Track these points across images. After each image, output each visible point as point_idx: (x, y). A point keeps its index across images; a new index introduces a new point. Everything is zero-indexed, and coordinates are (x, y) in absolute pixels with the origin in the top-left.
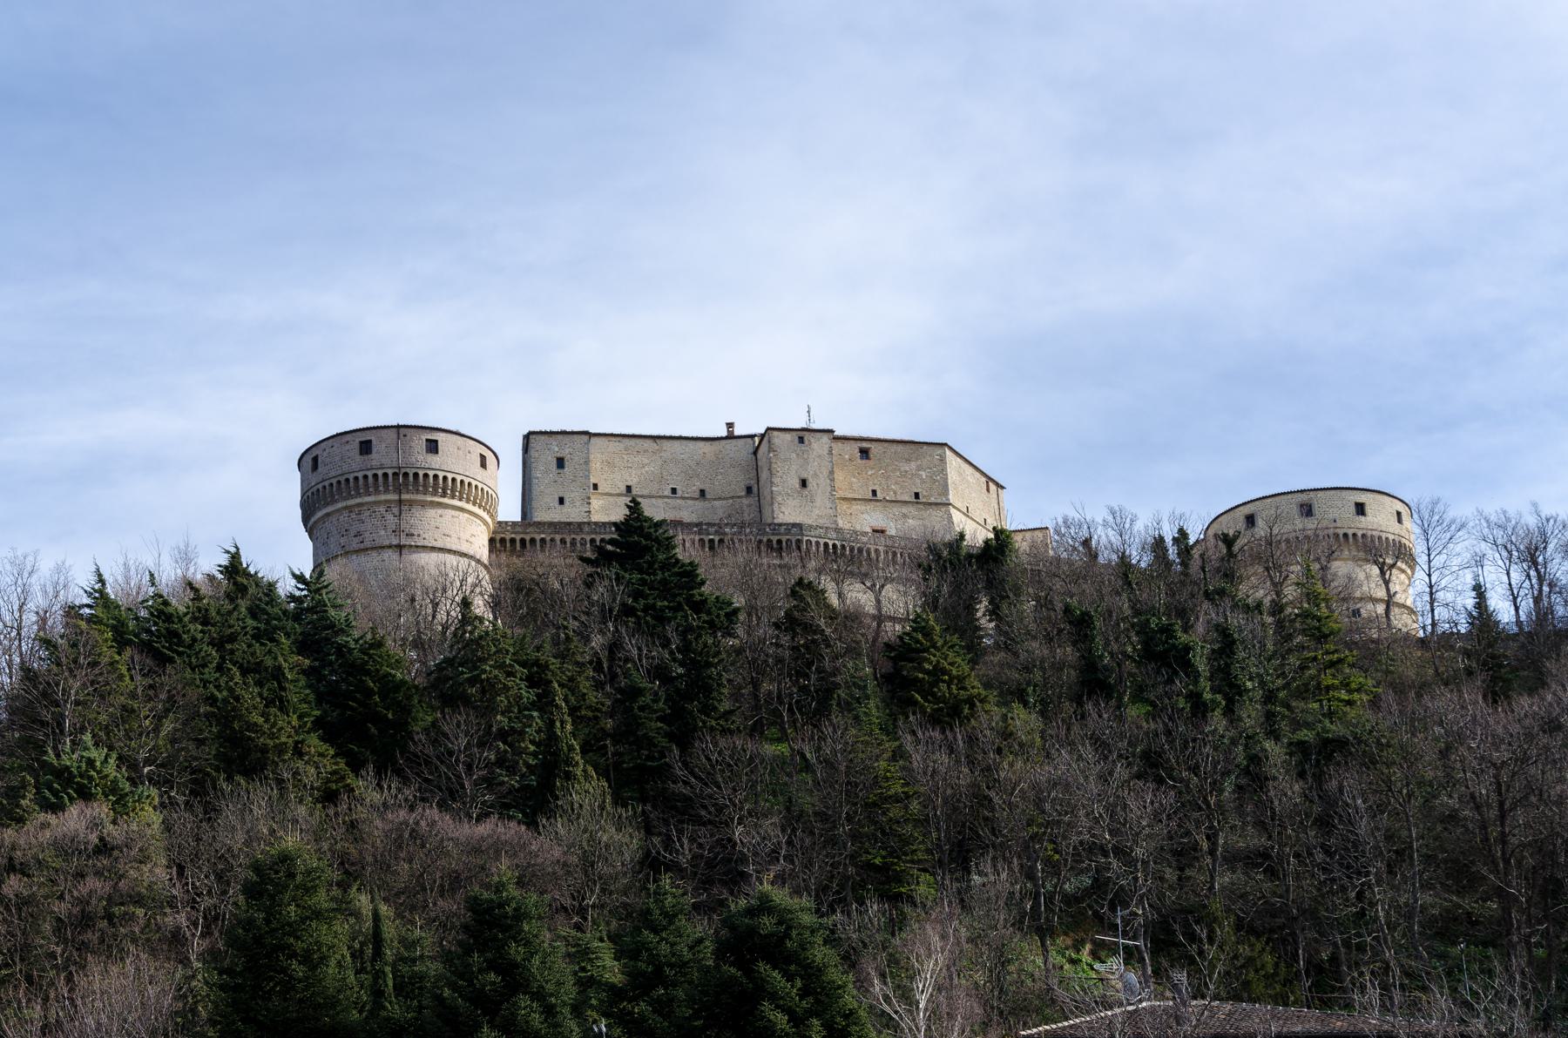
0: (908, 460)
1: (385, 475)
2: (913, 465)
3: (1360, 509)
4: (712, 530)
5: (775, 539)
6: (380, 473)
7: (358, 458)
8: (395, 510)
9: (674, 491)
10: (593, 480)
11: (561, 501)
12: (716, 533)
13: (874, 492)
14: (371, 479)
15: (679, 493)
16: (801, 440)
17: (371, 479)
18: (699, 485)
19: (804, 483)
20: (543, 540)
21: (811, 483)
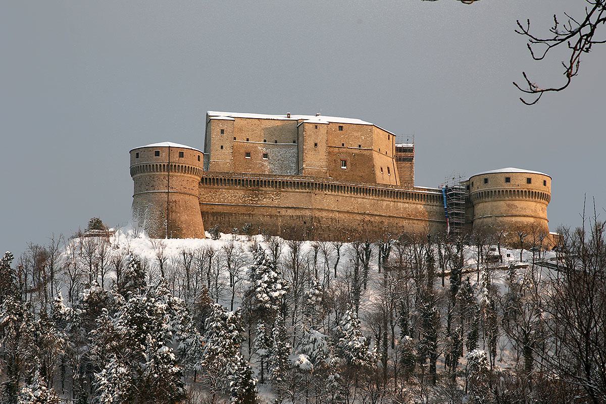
1: (164, 165)
2: (360, 133)
8: (167, 178)
11: (222, 147)
14: (159, 166)
16: (316, 127)
17: (159, 166)
19: (316, 145)
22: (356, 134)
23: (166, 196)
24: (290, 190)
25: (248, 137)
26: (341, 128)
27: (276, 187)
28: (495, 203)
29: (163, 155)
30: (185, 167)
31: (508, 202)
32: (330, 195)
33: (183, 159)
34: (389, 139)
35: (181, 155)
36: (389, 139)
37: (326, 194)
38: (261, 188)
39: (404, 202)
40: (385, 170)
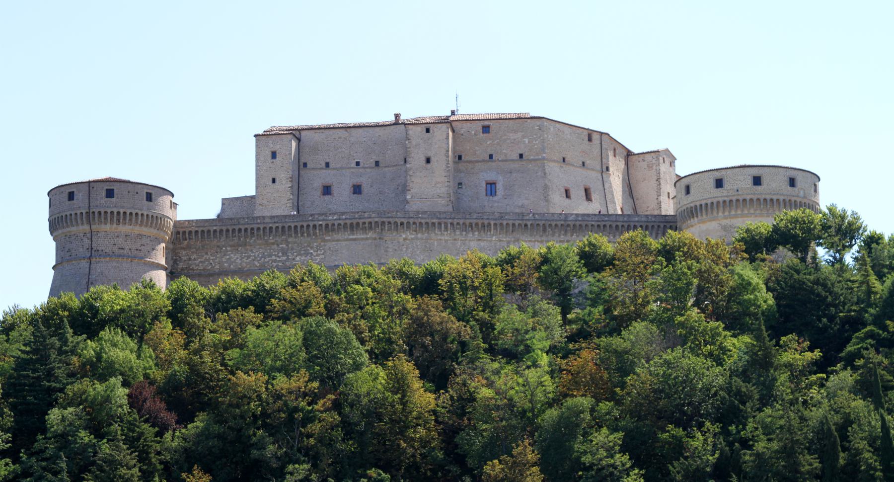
0: (516, 132)
2: (519, 135)
3: (757, 181)
4: (321, 218)
5: (361, 221)
6: (78, 213)
7: (68, 203)
8: (89, 235)
9: (358, 164)
10: (303, 161)
11: (274, 181)
12: (323, 220)
13: (491, 156)
15: (361, 165)
16: (428, 131)
18: (375, 158)
19: (428, 161)
20: (215, 231)
21: (433, 159)
22: (512, 136)
23: (87, 265)
24: (336, 236)
25: (328, 161)
26: (486, 129)
27: (315, 234)
28: (704, 227)
29: (79, 196)
30: (118, 213)
31: (725, 222)
32: (412, 239)
33: (113, 200)
34: (590, 139)
35: (110, 194)
36: (590, 139)
37: (405, 239)
38: (290, 240)
39: (561, 241)
40: (578, 194)
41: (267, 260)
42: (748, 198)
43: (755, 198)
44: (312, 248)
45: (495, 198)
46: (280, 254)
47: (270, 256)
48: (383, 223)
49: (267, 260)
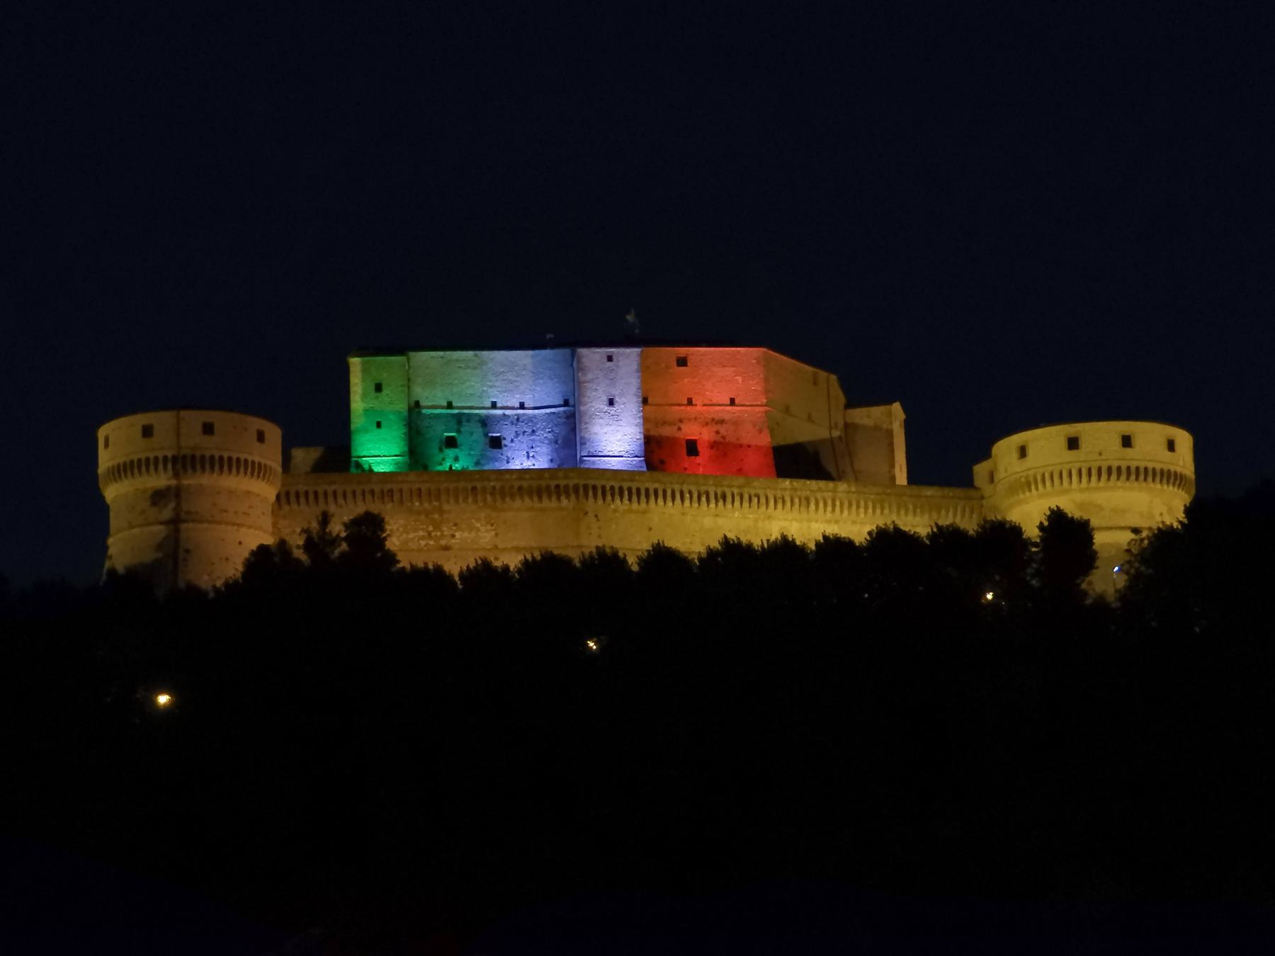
3: (1127, 441)
16: (610, 359)
34: (815, 383)
37: (615, 511)
38: (446, 507)
41: (411, 536)
42: (1115, 464)
43: (1124, 465)
44: (478, 520)
45: (699, 460)
46: (431, 528)
47: (416, 530)
48: (586, 487)
49: (411, 536)
